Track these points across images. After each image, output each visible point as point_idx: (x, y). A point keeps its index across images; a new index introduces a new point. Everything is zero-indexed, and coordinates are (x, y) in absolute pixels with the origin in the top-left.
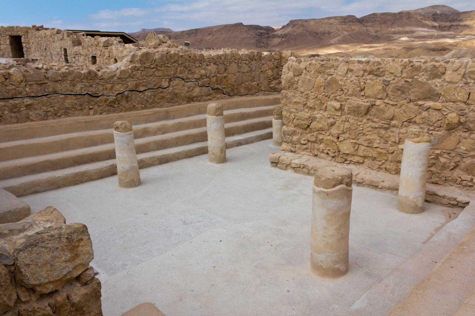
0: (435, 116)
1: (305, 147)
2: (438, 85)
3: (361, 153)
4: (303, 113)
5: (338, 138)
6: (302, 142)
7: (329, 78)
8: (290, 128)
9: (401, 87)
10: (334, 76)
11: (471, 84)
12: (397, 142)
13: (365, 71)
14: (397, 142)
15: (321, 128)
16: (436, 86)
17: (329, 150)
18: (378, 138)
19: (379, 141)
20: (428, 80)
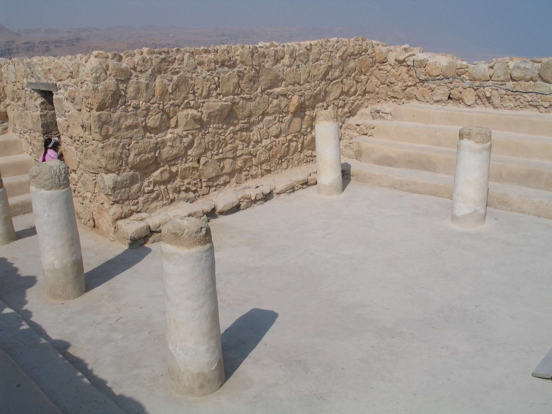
0: (284, 102)
1: (154, 195)
2: (281, 70)
3: (227, 169)
4: (146, 140)
5: (199, 161)
6: (147, 189)
7: (175, 77)
8: (125, 174)
9: (253, 77)
10: (181, 73)
11: (300, 66)
12: (259, 140)
13: (216, 62)
14: (259, 140)
15: (176, 155)
16: (280, 71)
17: (189, 183)
18: (240, 143)
19: (241, 146)
20: (273, 65)
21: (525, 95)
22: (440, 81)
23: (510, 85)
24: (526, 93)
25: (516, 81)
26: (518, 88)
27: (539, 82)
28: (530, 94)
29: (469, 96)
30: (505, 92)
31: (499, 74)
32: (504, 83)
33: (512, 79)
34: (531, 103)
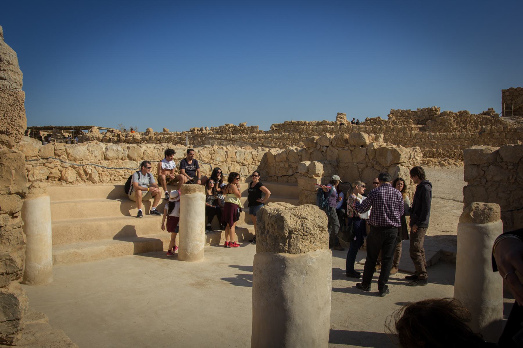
21: (119, 170)
22: (36, 162)
23: (105, 163)
24: (121, 168)
25: (108, 160)
26: (113, 166)
27: (127, 160)
28: (123, 170)
29: (71, 175)
30: (101, 169)
31: (97, 155)
32: (100, 162)
33: (106, 159)
34: (123, 176)
